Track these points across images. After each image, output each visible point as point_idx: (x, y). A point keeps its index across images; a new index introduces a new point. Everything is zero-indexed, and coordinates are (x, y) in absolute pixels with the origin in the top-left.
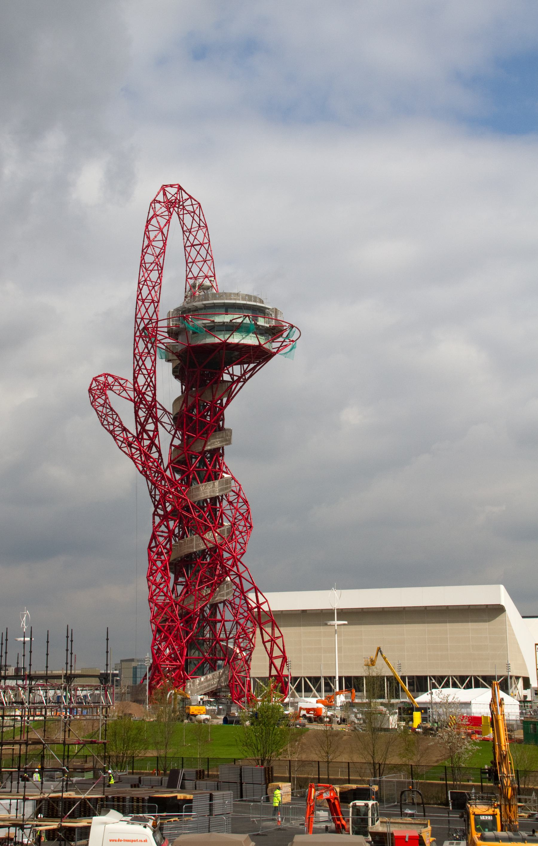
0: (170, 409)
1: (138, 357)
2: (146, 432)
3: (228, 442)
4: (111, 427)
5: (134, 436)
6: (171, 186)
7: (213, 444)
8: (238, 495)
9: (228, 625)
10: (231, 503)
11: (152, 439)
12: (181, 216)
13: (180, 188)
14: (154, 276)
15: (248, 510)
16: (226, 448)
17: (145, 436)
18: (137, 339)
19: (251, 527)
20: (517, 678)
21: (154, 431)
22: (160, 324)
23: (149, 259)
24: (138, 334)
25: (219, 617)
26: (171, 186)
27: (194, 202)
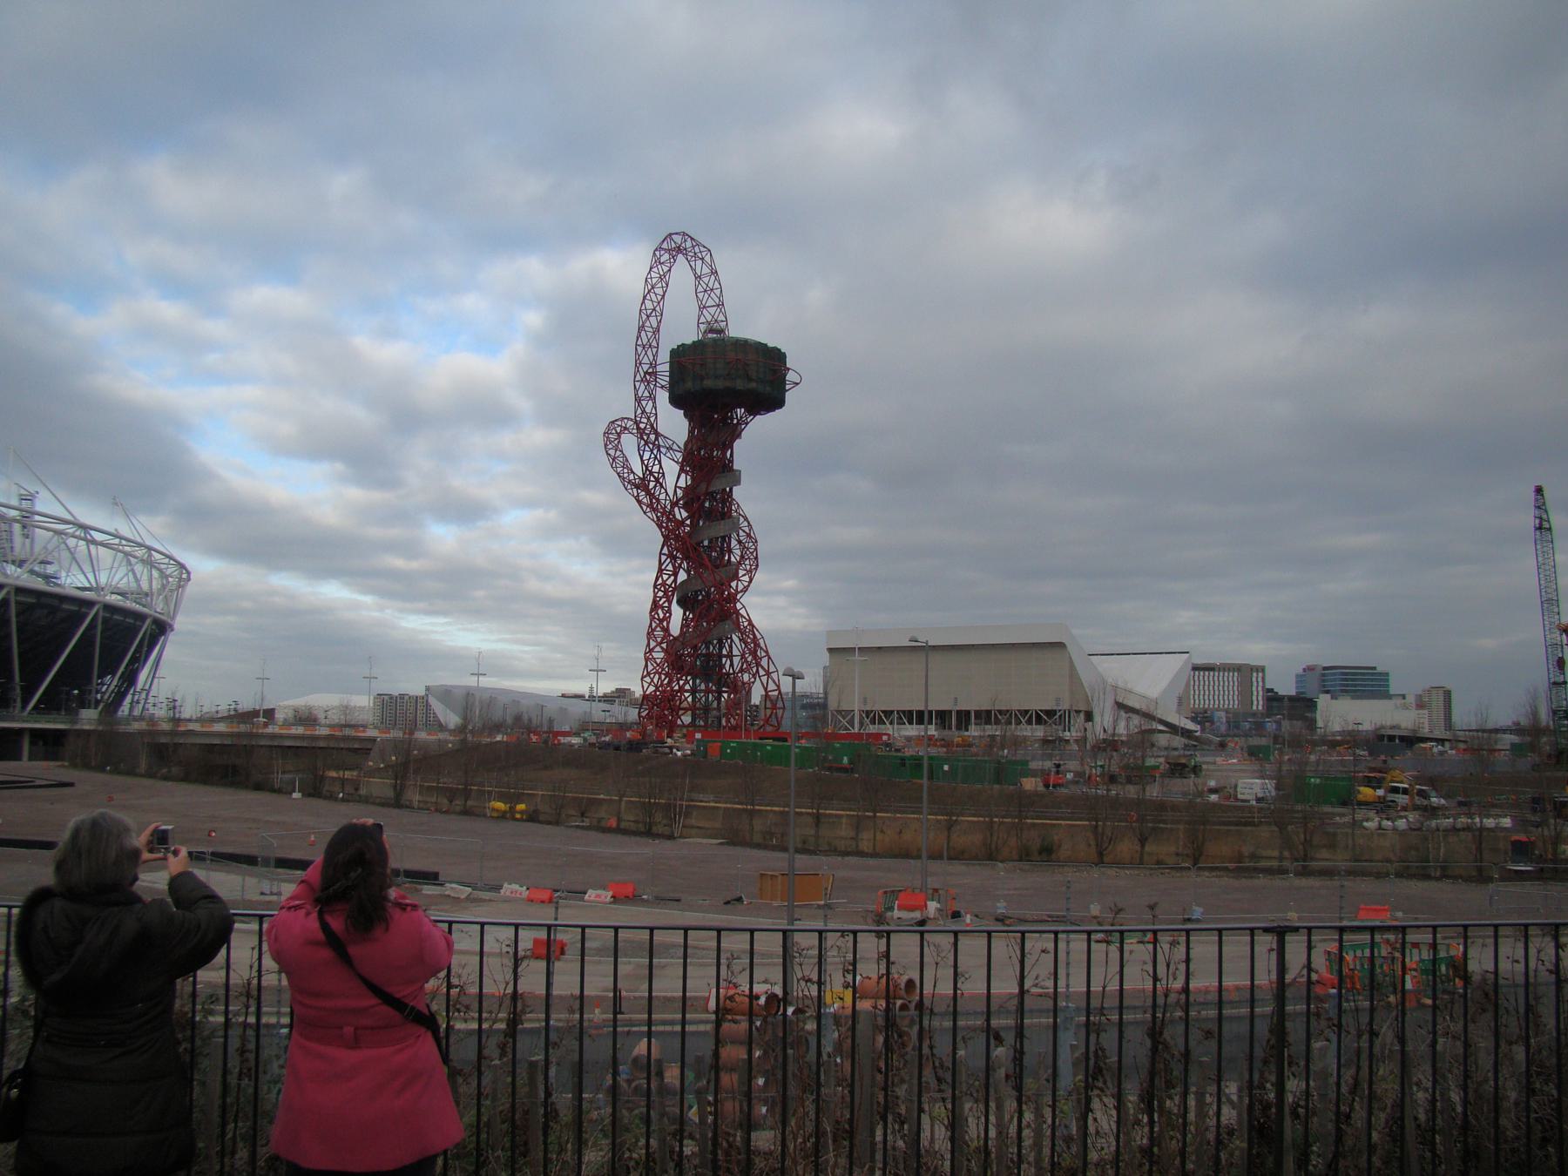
0: (682, 447)
1: (638, 400)
2: (651, 473)
3: (738, 482)
4: (619, 470)
5: (639, 478)
6: (676, 234)
7: (717, 485)
8: (748, 535)
9: (736, 660)
10: (740, 542)
11: (657, 480)
12: (693, 264)
13: (684, 234)
14: (653, 321)
15: (756, 549)
16: (734, 488)
17: (652, 479)
18: (637, 384)
19: (757, 566)
20: (1078, 712)
21: (659, 473)
22: (659, 368)
23: (649, 305)
24: (638, 378)
25: (724, 652)
26: (676, 234)
27: (702, 249)
